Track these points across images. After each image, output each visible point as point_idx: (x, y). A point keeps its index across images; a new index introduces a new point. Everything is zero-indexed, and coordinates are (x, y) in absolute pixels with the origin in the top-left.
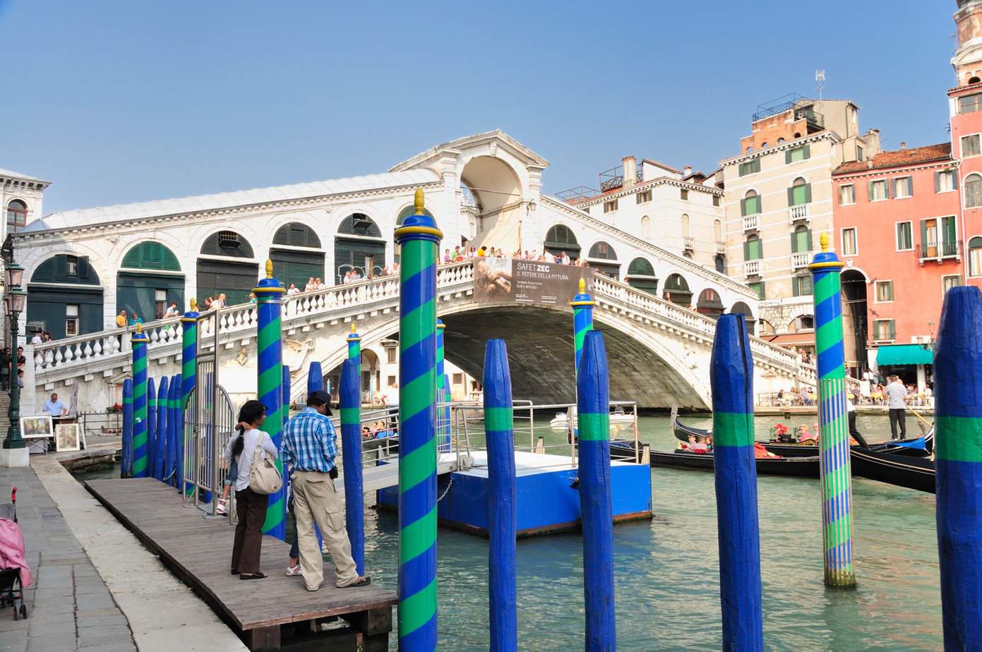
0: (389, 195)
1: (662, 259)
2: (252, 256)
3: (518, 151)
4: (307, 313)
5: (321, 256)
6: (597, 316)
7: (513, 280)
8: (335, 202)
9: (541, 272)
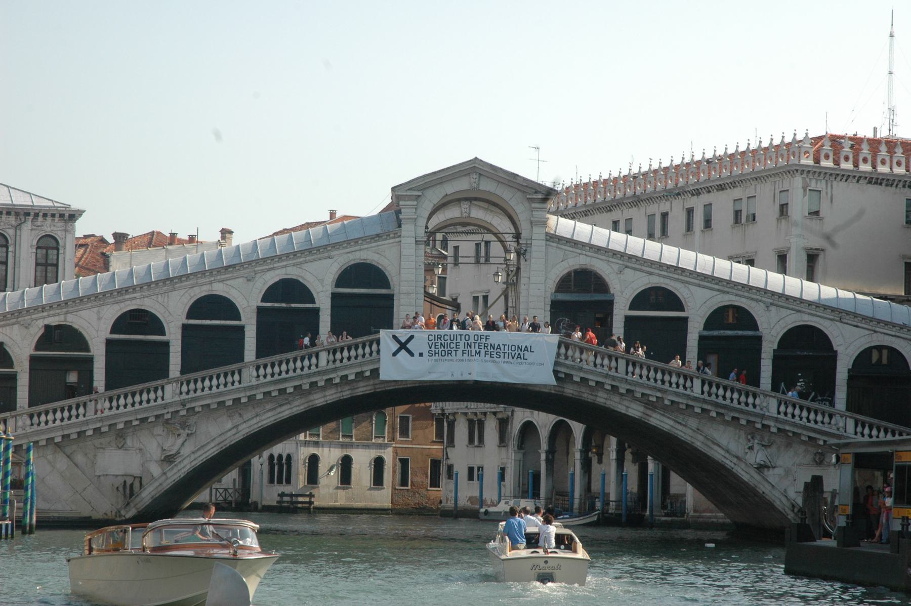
0: (326, 255)
1: (772, 304)
2: (163, 333)
4: (184, 396)
5: (241, 329)
6: (585, 395)
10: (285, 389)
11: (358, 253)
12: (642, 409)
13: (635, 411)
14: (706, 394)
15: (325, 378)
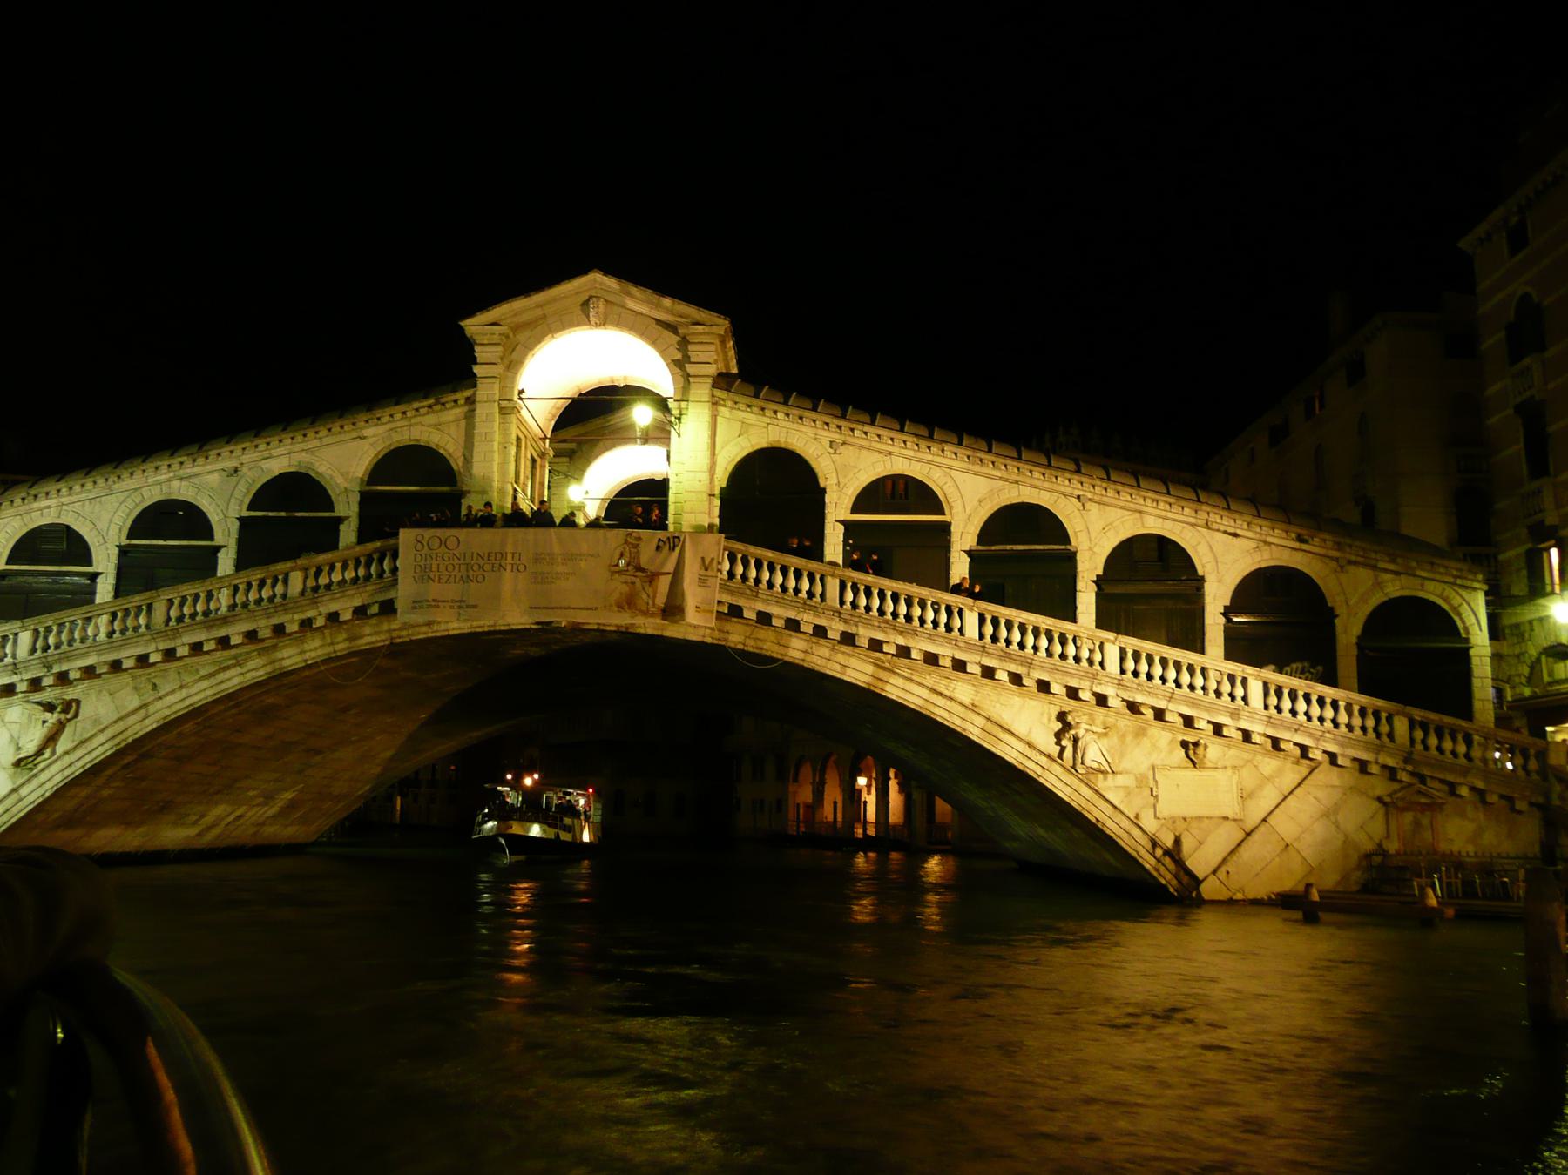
2: (90, 564)
12: (870, 669)
13: (856, 670)
14: (988, 640)
15: (297, 617)
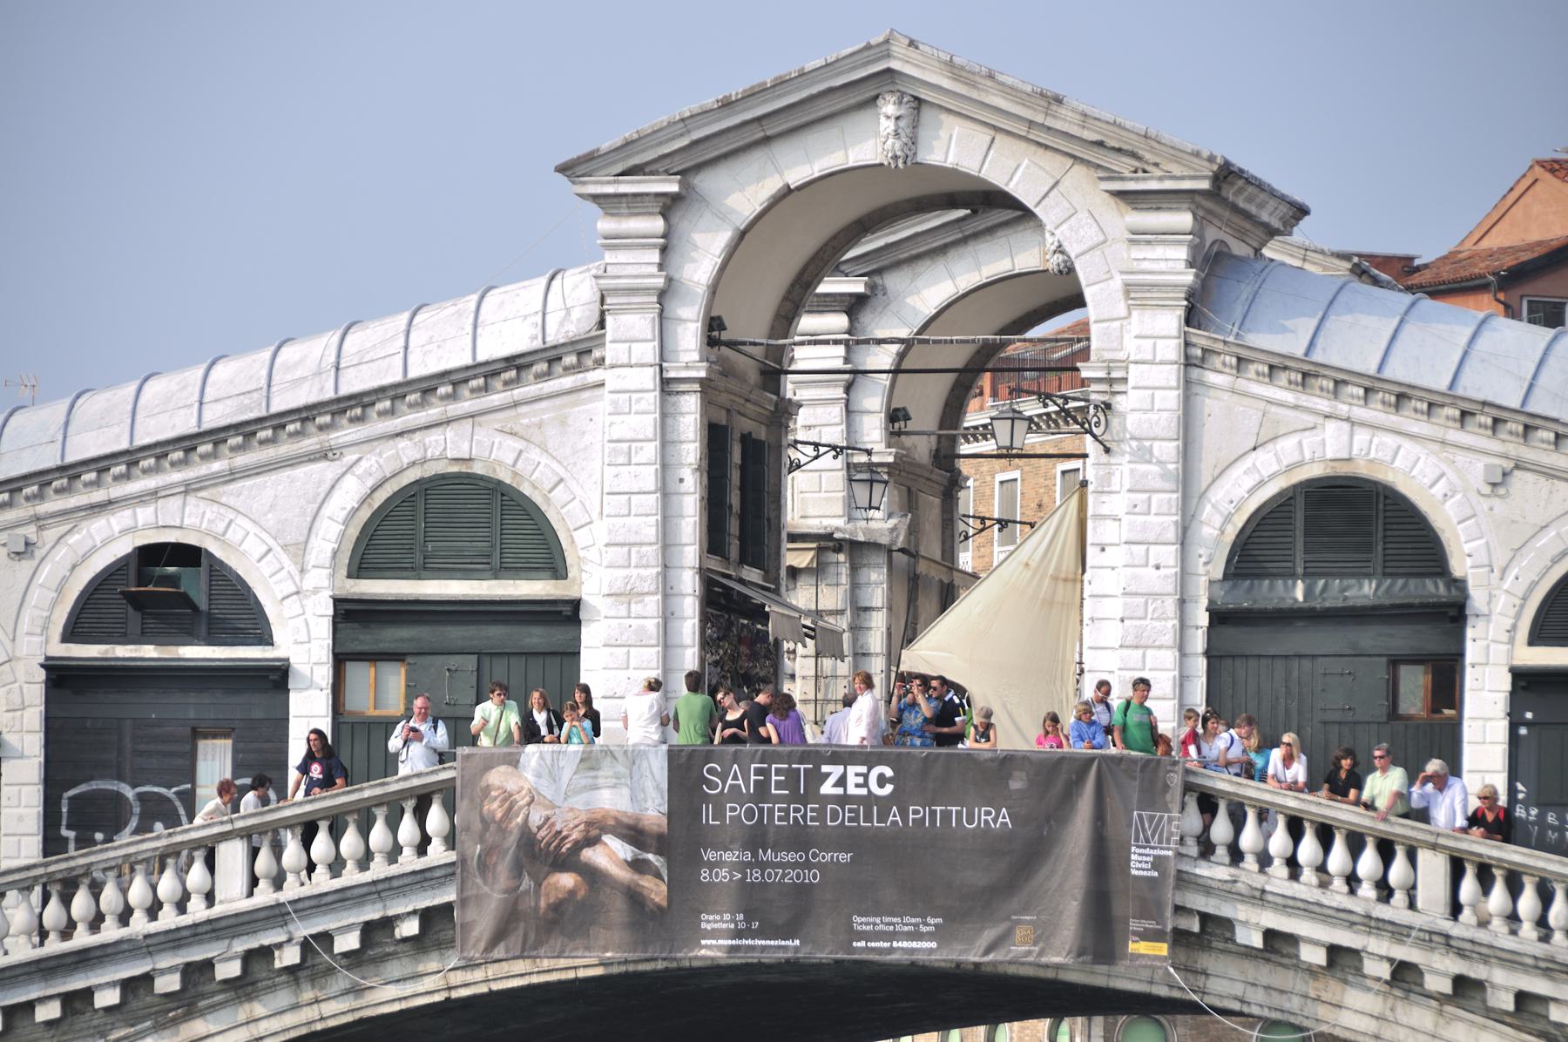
0: (310, 443)
3: (1031, 123)
6: (1294, 1003)
7: (677, 841)
8: (53, 504)
9: (844, 800)
10: (88, 993)
11: (434, 438)
